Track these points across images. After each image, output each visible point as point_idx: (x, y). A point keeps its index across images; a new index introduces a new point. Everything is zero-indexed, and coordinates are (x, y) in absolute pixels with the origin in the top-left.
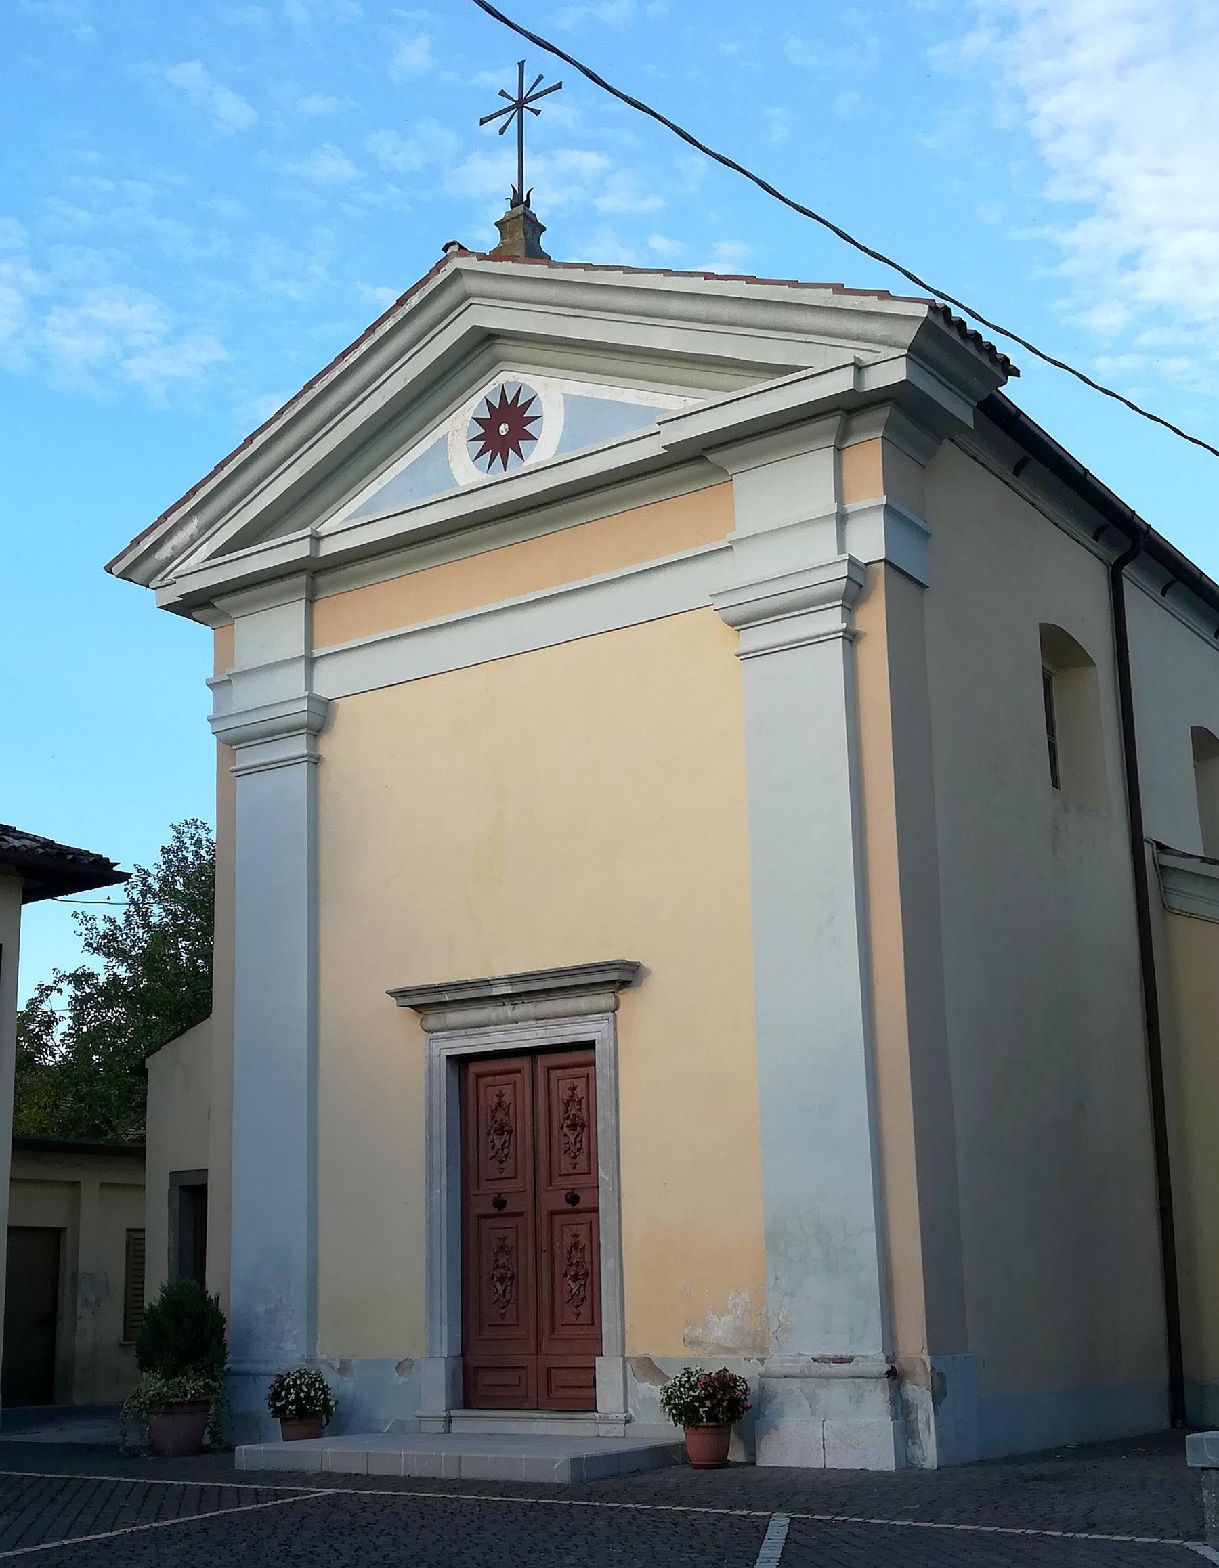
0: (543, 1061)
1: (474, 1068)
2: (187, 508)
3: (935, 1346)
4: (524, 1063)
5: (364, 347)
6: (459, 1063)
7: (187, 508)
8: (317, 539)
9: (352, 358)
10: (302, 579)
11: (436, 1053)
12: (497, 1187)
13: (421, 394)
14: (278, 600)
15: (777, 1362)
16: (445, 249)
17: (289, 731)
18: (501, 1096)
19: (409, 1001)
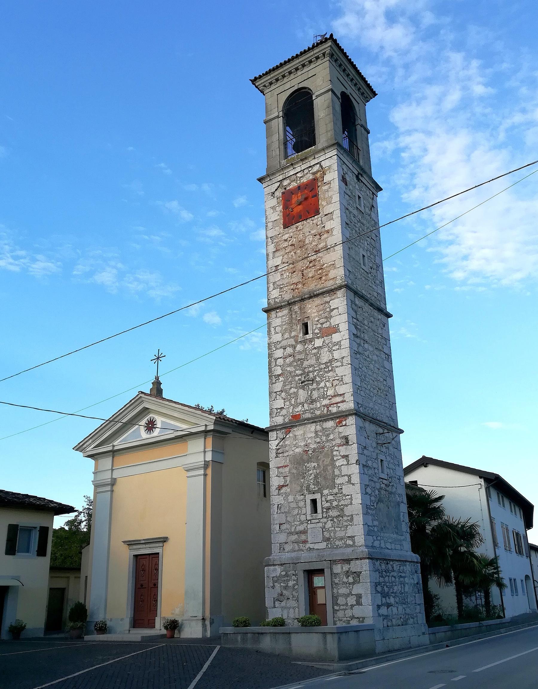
0: (151, 556)
1: (139, 557)
2: (89, 438)
3: (211, 614)
4: (148, 556)
5: (123, 409)
6: (136, 556)
7: (89, 438)
8: (114, 446)
9: (121, 411)
10: (111, 453)
11: (131, 554)
12: (142, 582)
13: (135, 418)
14: (107, 457)
15: (185, 618)
16: (139, 392)
17: (108, 485)
18: (143, 563)
19: (126, 543)
